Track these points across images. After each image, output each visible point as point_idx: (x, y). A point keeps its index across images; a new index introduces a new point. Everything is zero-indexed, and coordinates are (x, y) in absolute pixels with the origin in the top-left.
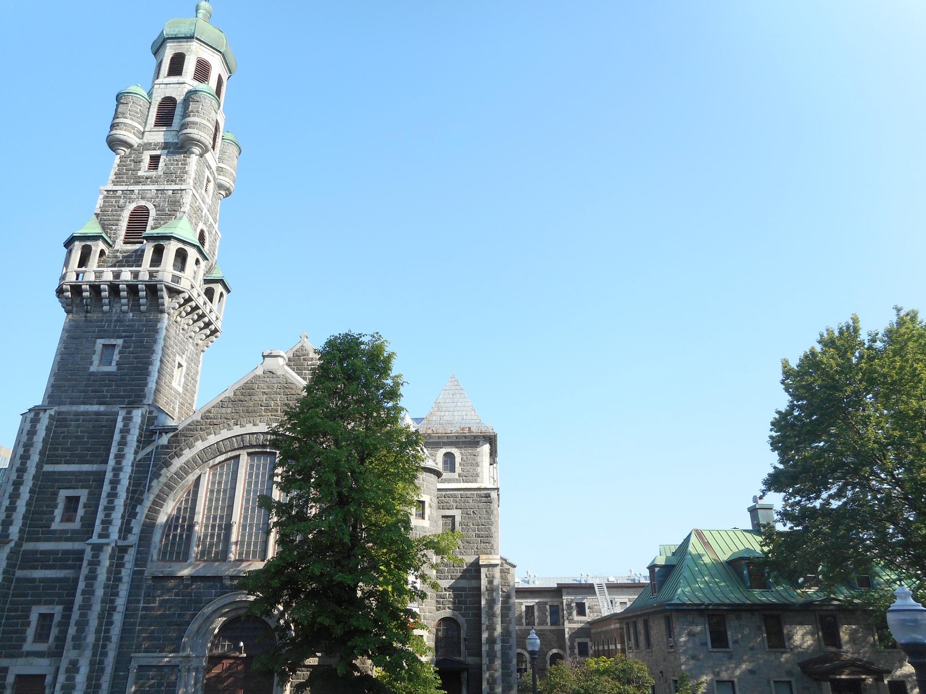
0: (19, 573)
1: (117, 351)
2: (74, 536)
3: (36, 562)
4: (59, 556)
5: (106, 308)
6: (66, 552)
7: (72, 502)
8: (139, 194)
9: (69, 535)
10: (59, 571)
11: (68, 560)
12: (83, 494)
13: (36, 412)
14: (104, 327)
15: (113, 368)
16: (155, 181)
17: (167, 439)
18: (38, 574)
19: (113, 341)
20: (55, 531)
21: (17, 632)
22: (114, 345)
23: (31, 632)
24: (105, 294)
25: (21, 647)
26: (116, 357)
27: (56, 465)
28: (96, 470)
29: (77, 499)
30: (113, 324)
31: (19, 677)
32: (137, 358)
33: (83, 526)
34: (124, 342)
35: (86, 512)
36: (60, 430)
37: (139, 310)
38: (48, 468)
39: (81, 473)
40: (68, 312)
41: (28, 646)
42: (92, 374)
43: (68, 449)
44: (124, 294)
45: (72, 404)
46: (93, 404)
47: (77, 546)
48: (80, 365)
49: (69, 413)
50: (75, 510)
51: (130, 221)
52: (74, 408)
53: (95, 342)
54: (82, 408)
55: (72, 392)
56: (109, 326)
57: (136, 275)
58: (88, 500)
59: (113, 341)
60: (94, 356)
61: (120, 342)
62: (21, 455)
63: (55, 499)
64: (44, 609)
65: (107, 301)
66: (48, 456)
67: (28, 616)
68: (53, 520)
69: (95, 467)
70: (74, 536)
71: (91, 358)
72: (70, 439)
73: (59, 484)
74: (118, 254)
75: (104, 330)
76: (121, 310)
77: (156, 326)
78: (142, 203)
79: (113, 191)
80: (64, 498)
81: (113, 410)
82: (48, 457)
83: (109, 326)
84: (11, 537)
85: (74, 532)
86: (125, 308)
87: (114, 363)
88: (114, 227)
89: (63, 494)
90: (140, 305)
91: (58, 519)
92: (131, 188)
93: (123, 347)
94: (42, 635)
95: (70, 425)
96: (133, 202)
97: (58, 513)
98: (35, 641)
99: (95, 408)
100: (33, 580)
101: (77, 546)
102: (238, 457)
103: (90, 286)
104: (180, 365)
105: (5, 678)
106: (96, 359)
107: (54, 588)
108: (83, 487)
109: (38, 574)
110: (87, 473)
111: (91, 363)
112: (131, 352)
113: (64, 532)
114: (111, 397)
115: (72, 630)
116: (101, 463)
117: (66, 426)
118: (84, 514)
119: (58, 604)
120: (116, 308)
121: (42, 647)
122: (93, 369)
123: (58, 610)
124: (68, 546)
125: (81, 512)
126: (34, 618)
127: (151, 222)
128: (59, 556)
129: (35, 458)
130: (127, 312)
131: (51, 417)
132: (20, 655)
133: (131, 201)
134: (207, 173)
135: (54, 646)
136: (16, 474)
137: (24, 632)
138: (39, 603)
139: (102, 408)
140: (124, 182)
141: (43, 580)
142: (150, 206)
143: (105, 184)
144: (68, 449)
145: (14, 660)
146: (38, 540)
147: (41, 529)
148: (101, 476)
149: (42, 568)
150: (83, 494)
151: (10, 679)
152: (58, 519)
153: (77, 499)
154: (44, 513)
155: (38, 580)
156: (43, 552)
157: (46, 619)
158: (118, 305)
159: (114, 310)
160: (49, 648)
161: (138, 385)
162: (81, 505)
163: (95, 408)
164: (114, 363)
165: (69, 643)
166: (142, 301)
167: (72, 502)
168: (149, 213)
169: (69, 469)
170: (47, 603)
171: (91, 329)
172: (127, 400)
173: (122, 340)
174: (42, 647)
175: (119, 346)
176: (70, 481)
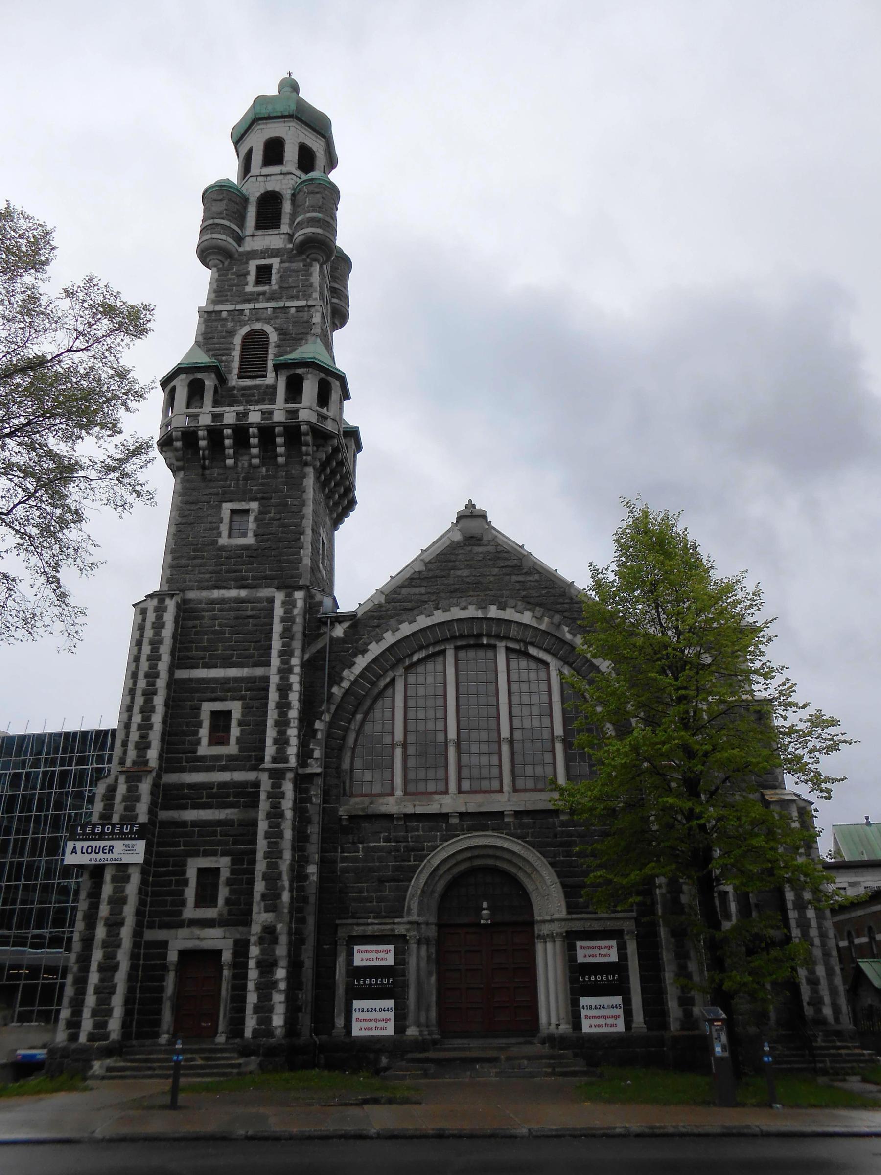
0: (164, 815)
1: (251, 518)
2: (231, 763)
4: (215, 790)
6: (223, 785)
9: (224, 763)
11: (228, 796)
15: (250, 540)
18: (190, 815)
19: (243, 506)
20: (203, 758)
21: (171, 893)
22: (246, 512)
23: (190, 893)
25: (180, 913)
26: (252, 525)
27: (192, 670)
28: (248, 675)
29: (228, 713)
31: (182, 953)
33: (240, 751)
35: (242, 731)
36: (190, 623)
39: (227, 680)
40: (175, 471)
41: (190, 912)
42: (223, 548)
43: (205, 649)
46: (230, 589)
48: (205, 537)
49: (200, 602)
50: (227, 729)
52: (205, 594)
53: (220, 507)
58: (243, 715)
59: (243, 506)
61: (254, 506)
63: (198, 715)
66: (179, 660)
67: (184, 873)
68: (198, 742)
69: (245, 672)
70: (231, 763)
71: (218, 528)
72: (206, 635)
73: (198, 695)
78: (258, 326)
80: (209, 713)
82: (179, 659)
83: (237, 485)
85: (230, 758)
86: (256, 461)
87: (250, 534)
88: (224, 358)
89: (207, 708)
90: (276, 456)
91: (205, 741)
92: (239, 307)
93: (261, 512)
94: (206, 898)
95: (203, 617)
96: (245, 325)
97: (204, 732)
98: (197, 905)
99: (233, 593)
100: (184, 824)
102: (443, 652)
105: (164, 956)
106: (224, 528)
107: (214, 833)
108: (233, 699)
109: (190, 815)
110: (236, 680)
113: (218, 758)
118: (241, 735)
119: (223, 855)
120: (244, 462)
121: (210, 913)
122: (224, 541)
123: (223, 863)
124: (225, 777)
126: (192, 874)
128: (215, 790)
130: (259, 467)
131: (178, 606)
132: (181, 925)
133: (243, 324)
137: (182, 893)
138: (196, 854)
139: (243, 593)
140: (227, 300)
141: (195, 824)
142: (268, 329)
144: (205, 649)
145: (173, 931)
146: (182, 770)
150: (236, 708)
151: (173, 956)
154: (185, 734)
155: (190, 823)
156: (192, 786)
157: (208, 876)
158: (246, 458)
159: (240, 464)
162: (234, 723)
163: (233, 593)
166: (280, 450)
168: (268, 338)
170: (206, 854)
171: (215, 490)
172: (276, 581)
175: (253, 510)
176: (214, 690)
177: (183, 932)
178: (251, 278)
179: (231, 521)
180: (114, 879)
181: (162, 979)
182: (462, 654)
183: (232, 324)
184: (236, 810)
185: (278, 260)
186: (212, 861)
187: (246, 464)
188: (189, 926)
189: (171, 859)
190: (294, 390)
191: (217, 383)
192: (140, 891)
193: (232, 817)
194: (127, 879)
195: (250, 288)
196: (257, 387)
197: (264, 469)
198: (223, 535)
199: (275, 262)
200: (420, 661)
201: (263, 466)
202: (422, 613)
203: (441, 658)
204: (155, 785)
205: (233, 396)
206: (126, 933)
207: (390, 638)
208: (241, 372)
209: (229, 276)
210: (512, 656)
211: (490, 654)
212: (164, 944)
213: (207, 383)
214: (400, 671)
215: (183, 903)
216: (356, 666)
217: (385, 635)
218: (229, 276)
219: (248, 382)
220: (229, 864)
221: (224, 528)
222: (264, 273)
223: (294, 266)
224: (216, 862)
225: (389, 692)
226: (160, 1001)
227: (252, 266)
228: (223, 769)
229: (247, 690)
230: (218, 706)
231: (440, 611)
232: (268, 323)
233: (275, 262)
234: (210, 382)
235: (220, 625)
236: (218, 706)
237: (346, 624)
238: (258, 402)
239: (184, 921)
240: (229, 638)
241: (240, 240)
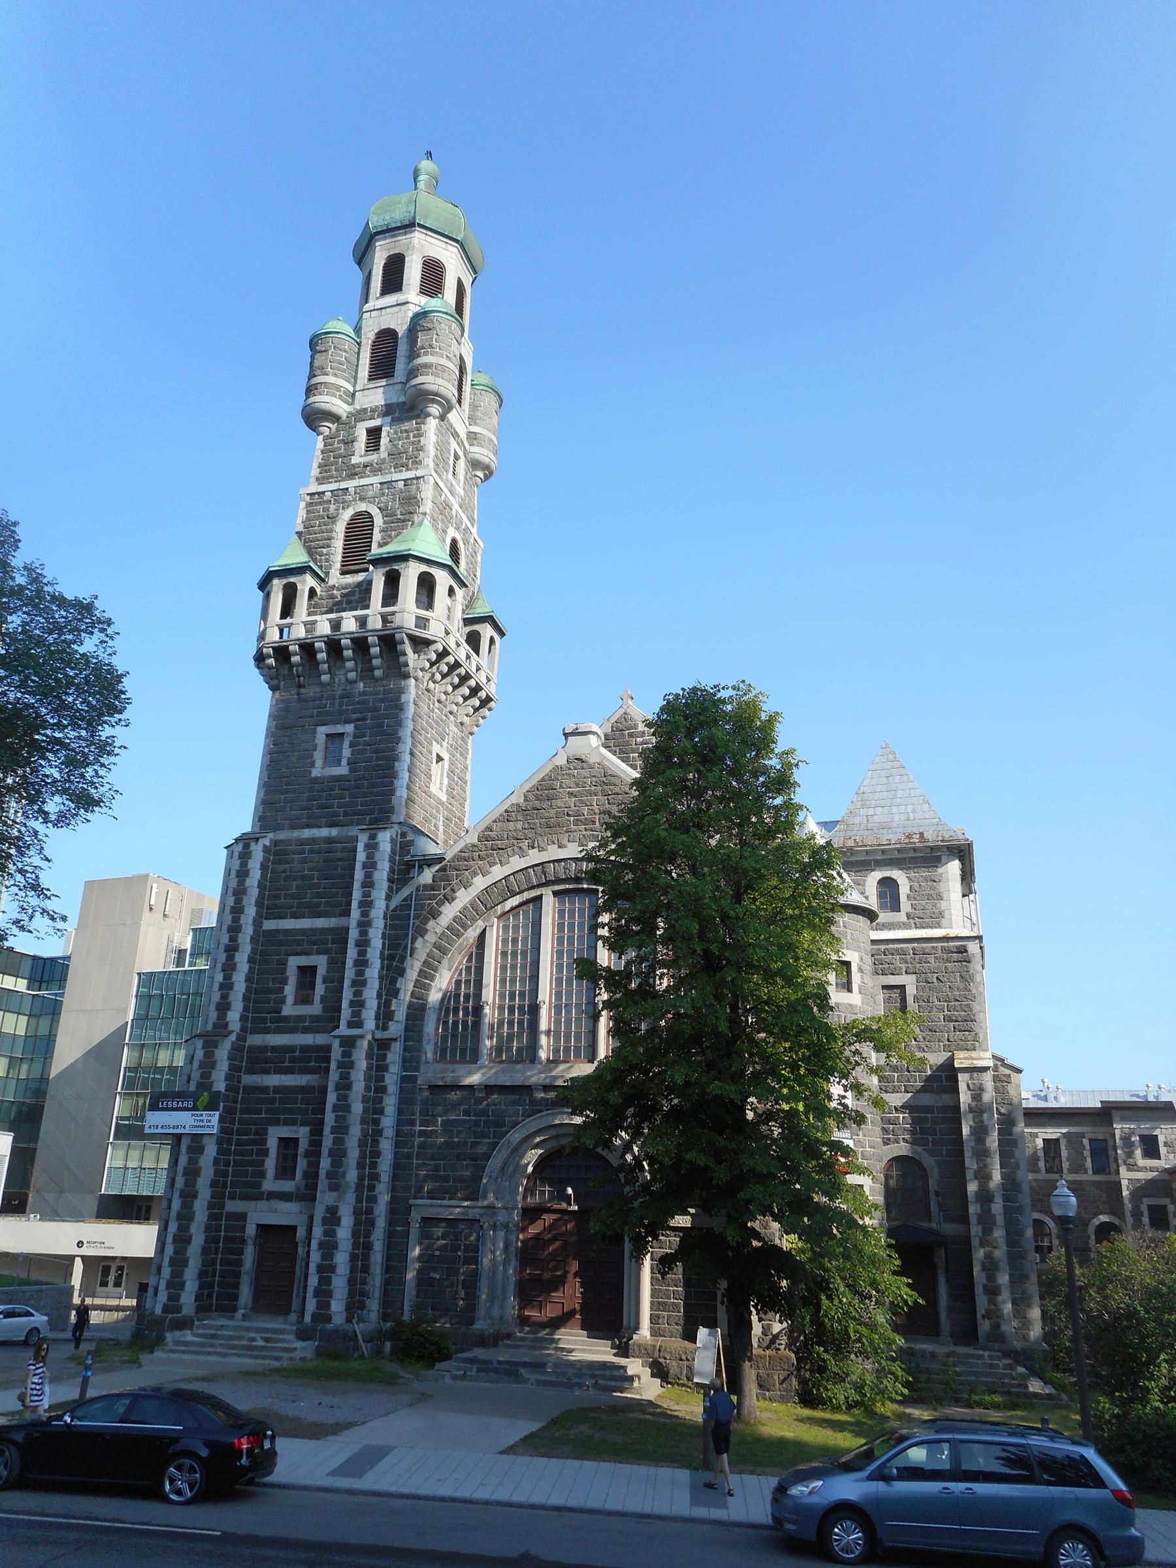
0: (248, 1079)
1: (346, 744)
3: (267, 1063)
4: (297, 1054)
5: (325, 678)
6: (305, 1049)
7: (307, 973)
8: (355, 493)
10: (298, 1077)
12: (321, 962)
13: (245, 841)
15: (343, 770)
16: (377, 469)
17: (431, 876)
18: (273, 1080)
19: (339, 729)
20: (287, 1019)
21: (250, 1163)
23: (270, 1164)
24: (322, 656)
25: (259, 1185)
26: (347, 752)
29: (313, 969)
30: (337, 701)
31: (262, 1228)
32: (376, 751)
33: (324, 1010)
35: (326, 988)
36: (280, 868)
37: (373, 677)
38: (269, 925)
39: (314, 931)
40: (273, 689)
41: (270, 1184)
42: (316, 780)
43: (292, 896)
44: (348, 653)
45: (292, 827)
47: (320, 1039)
49: (289, 842)
50: (312, 986)
51: (347, 538)
52: (296, 834)
53: (314, 732)
54: (307, 833)
55: (291, 810)
56: (332, 704)
57: (362, 622)
58: (328, 972)
59: (339, 729)
61: (349, 728)
62: (232, 907)
63: (284, 971)
64: (285, 1132)
65: (325, 666)
66: (269, 907)
67: (264, 1142)
68: (283, 1001)
71: (312, 756)
72: (295, 880)
74: (335, 592)
75: (326, 712)
76: (347, 679)
77: (399, 699)
78: (362, 507)
79: (319, 493)
80: (295, 969)
81: (350, 834)
82: (268, 908)
83: (332, 704)
84: (230, 1028)
85: (314, 1019)
86: (352, 675)
87: (344, 762)
88: (325, 551)
89: (294, 962)
90: (372, 669)
91: (290, 1000)
92: (343, 485)
93: (355, 736)
94: (285, 1170)
96: (348, 507)
97: (290, 990)
98: (277, 1178)
99: (324, 832)
100: (265, 1089)
101: (320, 1039)
102: (540, 898)
103: (300, 646)
104: (439, 759)
105: (243, 1228)
106: (318, 756)
108: (319, 953)
109: (273, 1080)
110: (323, 931)
111: (313, 764)
112: (367, 744)
113: (301, 1018)
114: (346, 814)
115: (325, 1163)
116: (340, 916)
117: (287, 862)
120: (340, 677)
121: (288, 1186)
122: (316, 772)
124: (307, 1039)
125: (320, 989)
126: (272, 1144)
127: (377, 536)
128: (297, 1054)
129: (251, 911)
131: (266, 849)
132: (259, 1197)
133: (346, 505)
134: (454, 445)
136: (228, 936)
137: (262, 1163)
138: (276, 1122)
139: (334, 832)
140: (332, 477)
141: (278, 1090)
142: (374, 511)
143: (307, 485)
144: (292, 896)
145: (253, 1203)
146: (266, 1031)
147: (269, 1016)
148: (341, 935)
149: (276, 1073)
150: (321, 962)
151: (251, 1231)
152: (290, 1000)
153: (313, 969)
154: (271, 991)
156: (275, 1049)
157: (288, 1144)
158: (342, 672)
159: (337, 680)
160: (298, 1188)
161: (382, 794)
163: (324, 832)
164: (344, 762)
165: (323, 1182)
166: (376, 662)
167: (307, 973)
168: (373, 521)
169: (298, 927)
170: (287, 1122)
171: (308, 712)
172: (368, 817)
173: (352, 725)
174: (288, 1186)
176: (300, 943)
177: (262, 1205)
179: (327, 748)
180: (190, 1150)
181: (241, 1252)
183: (335, 507)
186: (290, 1131)
187: (343, 679)
188: (268, 1199)
193: (312, 1083)
197: (362, 685)
201: (361, 680)
204: (236, 1049)
206: (200, 1207)
212: (243, 1217)
215: (263, 1175)
220: (308, 1134)
221: (318, 756)
224: (296, 1132)
226: (237, 1275)
228: (306, 1030)
229: (333, 943)
230: (304, 961)
235: (309, 870)
236: (304, 961)
239: (263, 1193)
240: (318, 884)
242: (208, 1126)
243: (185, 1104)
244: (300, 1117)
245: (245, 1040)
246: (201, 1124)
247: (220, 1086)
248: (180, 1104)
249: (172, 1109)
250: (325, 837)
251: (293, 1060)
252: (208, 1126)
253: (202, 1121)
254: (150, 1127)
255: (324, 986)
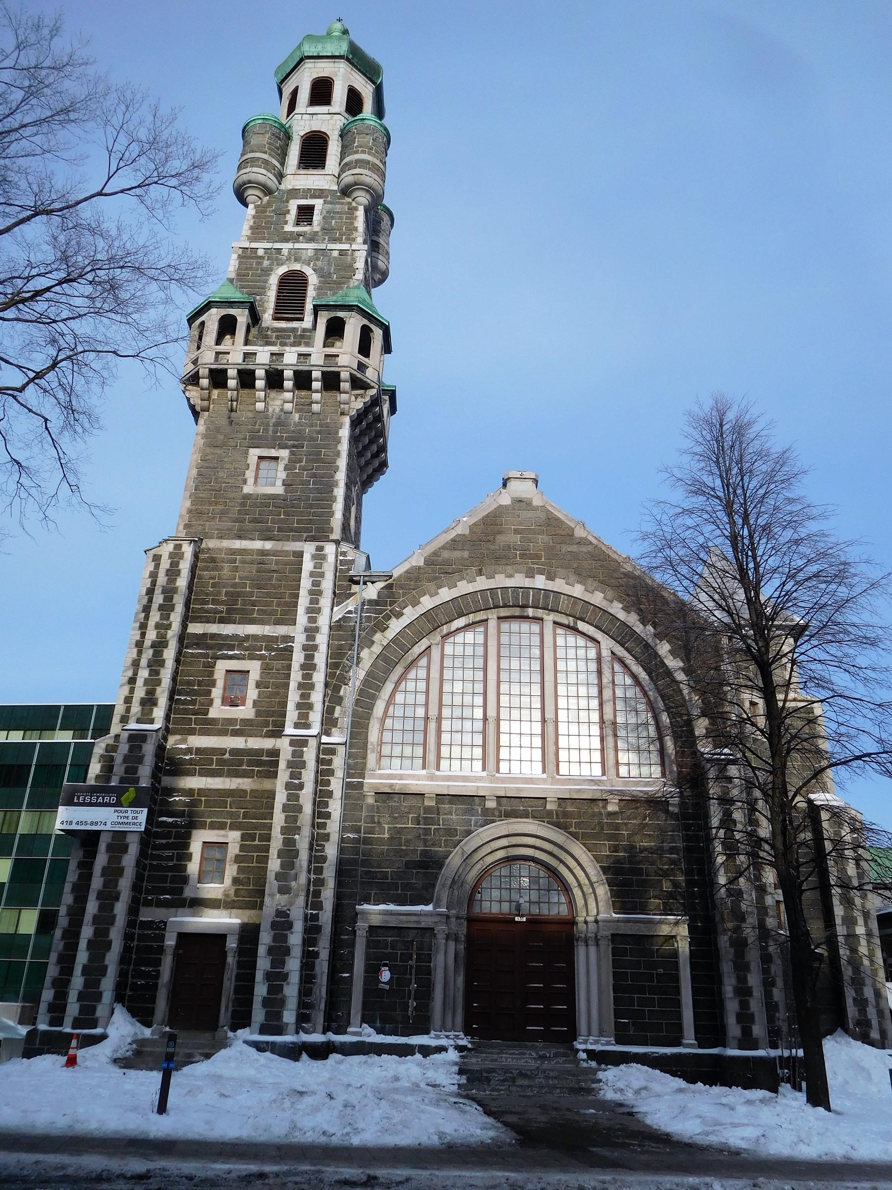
2: (244, 729)
4: (227, 756)
6: (234, 752)
9: (238, 727)
10: (228, 780)
11: (241, 763)
14: (259, 431)
19: (273, 453)
20: (214, 721)
22: (276, 459)
30: (271, 428)
32: (314, 476)
34: (292, 453)
37: (310, 411)
38: (195, 628)
42: (247, 496)
46: (254, 540)
48: (228, 483)
52: (226, 544)
54: (238, 544)
56: (266, 430)
58: (261, 677)
59: (273, 453)
60: (247, 472)
61: (284, 453)
63: (211, 673)
69: (266, 630)
70: (244, 729)
76: (282, 410)
77: (337, 432)
81: (284, 549)
85: (244, 721)
87: (279, 483)
89: (222, 667)
91: (217, 702)
99: (258, 545)
106: (250, 475)
111: (245, 482)
112: (303, 469)
113: (231, 721)
117: (215, 569)
119: (231, 829)
122: (248, 489)
123: (233, 838)
124: (238, 743)
128: (227, 756)
135: (232, 892)
139: (268, 545)
149: (201, 775)
150: (254, 668)
152: (217, 702)
161: (321, 515)
162: (251, 684)
163: (258, 545)
170: (213, 826)
172: (305, 535)
175: (283, 459)
178: (292, 216)
179: (258, 468)
180: (110, 848)
182: (505, 626)
184: (250, 780)
185: (321, 201)
186: (218, 836)
189: (174, 830)
190: (335, 330)
191: (250, 321)
192: (138, 863)
193: (244, 787)
194: (125, 849)
195: (289, 228)
196: (294, 330)
198: (248, 483)
199: (318, 203)
200: (458, 630)
202: (463, 579)
203: (482, 629)
205: (267, 336)
207: (427, 603)
208: (276, 313)
209: (268, 213)
210: (560, 631)
211: (536, 628)
213: (239, 319)
214: (436, 637)
216: (389, 630)
217: (422, 599)
218: (268, 213)
219: (283, 325)
222: (305, 213)
223: (338, 208)
224: (224, 836)
225: (423, 662)
227: (293, 206)
228: (236, 733)
231: (484, 577)
232: (309, 265)
233: (318, 203)
234: (242, 317)
237: (380, 585)
238: (294, 345)
241: (280, 176)
242: (134, 824)
243: (107, 799)
244: (229, 821)
245: (165, 739)
246: (126, 820)
247: (144, 783)
248: (100, 800)
249: (91, 804)
250: (259, 550)
251: (221, 762)
252: (134, 824)
253: (127, 818)
254: (62, 823)
255: (257, 691)
